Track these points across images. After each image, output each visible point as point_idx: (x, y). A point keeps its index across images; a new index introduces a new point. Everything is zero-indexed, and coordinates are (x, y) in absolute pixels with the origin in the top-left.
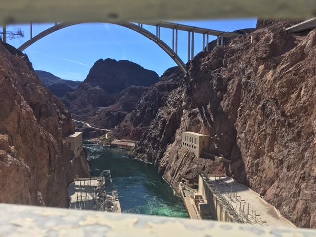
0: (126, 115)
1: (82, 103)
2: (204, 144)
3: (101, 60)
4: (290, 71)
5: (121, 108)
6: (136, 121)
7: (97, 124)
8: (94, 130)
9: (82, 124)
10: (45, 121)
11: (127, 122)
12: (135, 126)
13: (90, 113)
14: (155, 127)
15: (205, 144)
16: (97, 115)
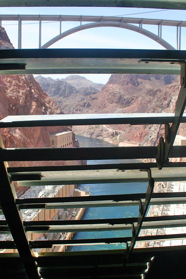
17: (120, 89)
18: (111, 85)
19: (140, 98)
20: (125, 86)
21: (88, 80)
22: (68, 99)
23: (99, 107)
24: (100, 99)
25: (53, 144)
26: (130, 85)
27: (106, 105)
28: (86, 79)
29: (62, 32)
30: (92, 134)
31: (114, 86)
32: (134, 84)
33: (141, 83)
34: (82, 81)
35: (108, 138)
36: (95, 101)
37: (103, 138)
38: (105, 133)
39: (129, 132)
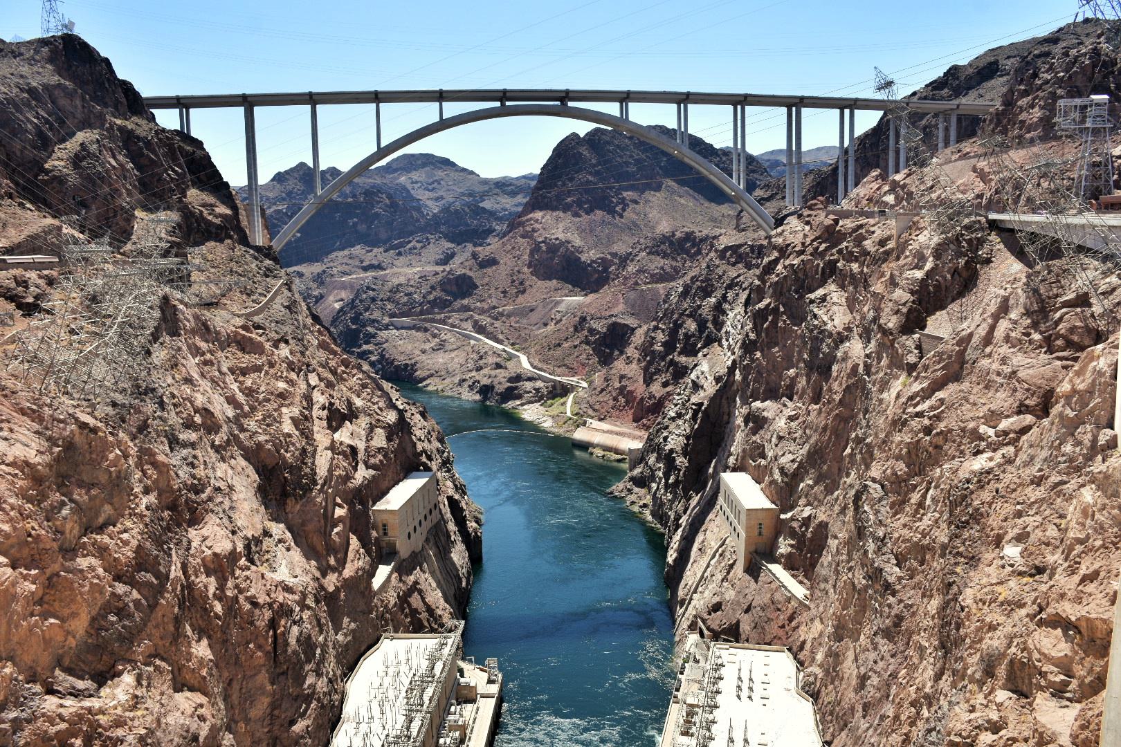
0: (634, 329)
1: (513, 281)
2: (760, 534)
3: (574, 135)
4: (919, 415)
5: (621, 307)
6: (652, 362)
7: (545, 361)
8: (540, 378)
9: (510, 357)
10: (298, 507)
11: (629, 361)
12: (648, 381)
13: (534, 317)
14: (679, 416)
15: (764, 531)
16: (551, 327)
17: (566, 230)
18: (538, 215)
19: (631, 268)
20: (585, 219)
21: (464, 170)
22: (400, 254)
23: (504, 292)
24: (506, 263)
25: (385, 534)
26: (599, 214)
27: (527, 284)
28: (453, 164)
29: (383, 144)
30: (486, 391)
31: (548, 217)
32: (612, 212)
33: (636, 202)
34: (440, 174)
35: (537, 405)
36: (489, 271)
37: (522, 405)
38: (528, 385)
39: (603, 390)
